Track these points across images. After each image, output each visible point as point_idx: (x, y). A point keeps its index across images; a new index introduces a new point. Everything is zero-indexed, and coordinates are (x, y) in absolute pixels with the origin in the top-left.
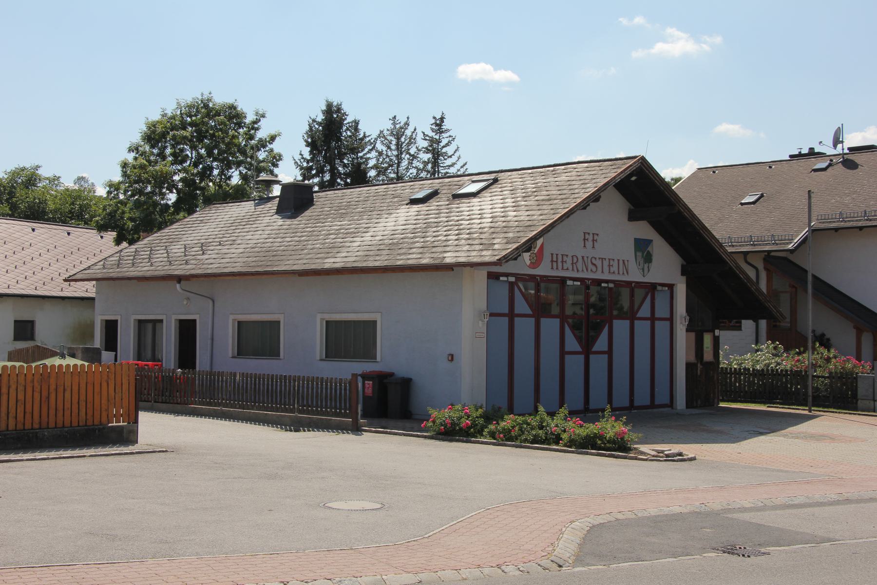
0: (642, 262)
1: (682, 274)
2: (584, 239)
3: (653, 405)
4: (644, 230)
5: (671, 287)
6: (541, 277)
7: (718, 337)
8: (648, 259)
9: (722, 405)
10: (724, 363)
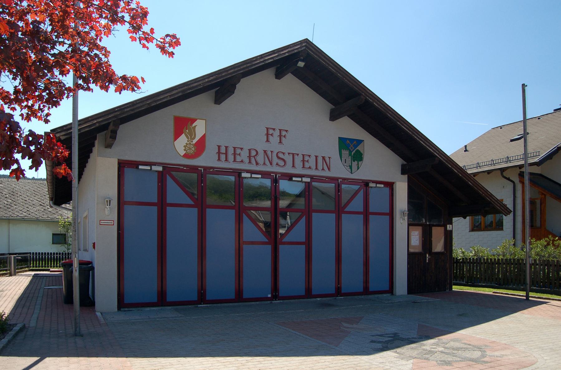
0: (349, 160)
1: (403, 173)
2: (267, 134)
3: (366, 291)
4: (349, 128)
5: (390, 185)
6: (205, 168)
7: (451, 232)
8: (358, 157)
9: (455, 288)
10: (458, 252)
